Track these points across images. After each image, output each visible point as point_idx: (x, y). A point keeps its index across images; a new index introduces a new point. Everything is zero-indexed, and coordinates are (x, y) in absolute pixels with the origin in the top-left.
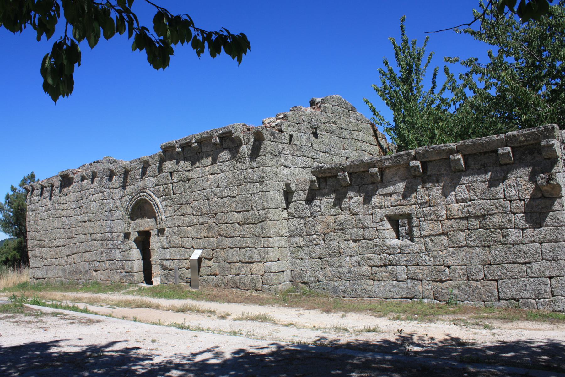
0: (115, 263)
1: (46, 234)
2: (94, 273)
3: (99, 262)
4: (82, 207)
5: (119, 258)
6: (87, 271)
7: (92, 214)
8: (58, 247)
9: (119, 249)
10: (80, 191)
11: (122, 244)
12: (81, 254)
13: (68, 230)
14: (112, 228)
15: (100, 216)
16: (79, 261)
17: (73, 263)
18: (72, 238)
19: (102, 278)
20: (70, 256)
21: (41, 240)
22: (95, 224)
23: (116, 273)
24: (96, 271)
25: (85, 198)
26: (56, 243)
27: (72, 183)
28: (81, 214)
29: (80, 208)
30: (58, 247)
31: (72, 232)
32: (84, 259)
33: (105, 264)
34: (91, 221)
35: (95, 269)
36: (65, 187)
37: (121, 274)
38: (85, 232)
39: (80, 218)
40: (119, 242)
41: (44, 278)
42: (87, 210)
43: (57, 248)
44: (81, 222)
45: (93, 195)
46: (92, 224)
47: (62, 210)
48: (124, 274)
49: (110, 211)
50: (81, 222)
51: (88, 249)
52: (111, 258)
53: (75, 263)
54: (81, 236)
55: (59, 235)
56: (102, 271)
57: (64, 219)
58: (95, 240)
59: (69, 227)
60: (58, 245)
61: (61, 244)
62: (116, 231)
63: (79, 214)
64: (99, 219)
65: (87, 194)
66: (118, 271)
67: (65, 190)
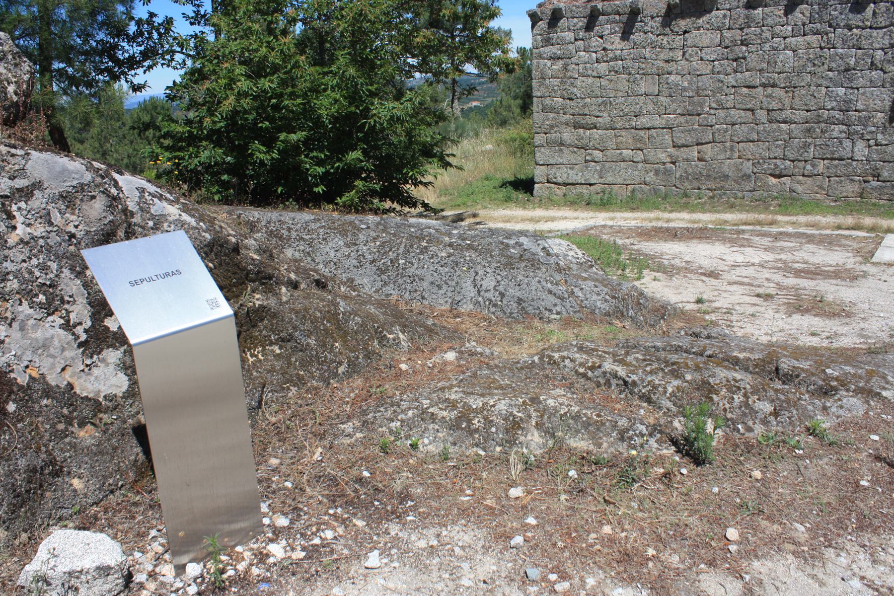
0: (851, 165)
1: (604, 103)
2: (773, 181)
3: (793, 161)
4: (744, 58)
5: (864, 156)
6: (750, 176)
7: (779, 73)
8: (649, 129)
9: (869, 140)
10: (741, 29)
11: (882, 133)
12: (728, 144)
13: (687, 99)
14: (848, 102)
15: (808, 78)
16: (722, 157)
17: (696, 159)
18: (699, 115)
19: (799, 188)
20: (687, 146)
21: (586, 115)
22: (787, 92)
23: (848, 182)
24: (780, 176)
25: (759, 41)
26: (644, 121)
27: (710, 12)
28: (736, 72)
29: (735, 60)
30: (649, 129)
31: (701, 105)
32: (736, 155)
33: (813, 166)
34: (774, 86)
35: (778, 172)
36: (683, 18)
37: (864, 185)
38: (748, 106)
39: (731, 80)
40: (873, 129)
41: (591, 185)
42: (765, 65)
43: (642, 133)
44: (734, 87)
45: (785, 38)
46: (778, 92)
47: (667, 61)
48: (875, 184)
49: (847, 70)
50: (734, 87)
51: (755, 136)
52: (836, 156)
53: (700, 160)
54: (733, 112)
55: (651, 107)
56: (801, 178)
57: (672, 78)
58: (785, 122)
59: (691, 94)
60: (648, 125)
61: (658, 121)
62: (860, 106)
63: (729, 70)
64: (803, 84)
65: (768, 35)
66: (857, 178)
67: (683, 24)
